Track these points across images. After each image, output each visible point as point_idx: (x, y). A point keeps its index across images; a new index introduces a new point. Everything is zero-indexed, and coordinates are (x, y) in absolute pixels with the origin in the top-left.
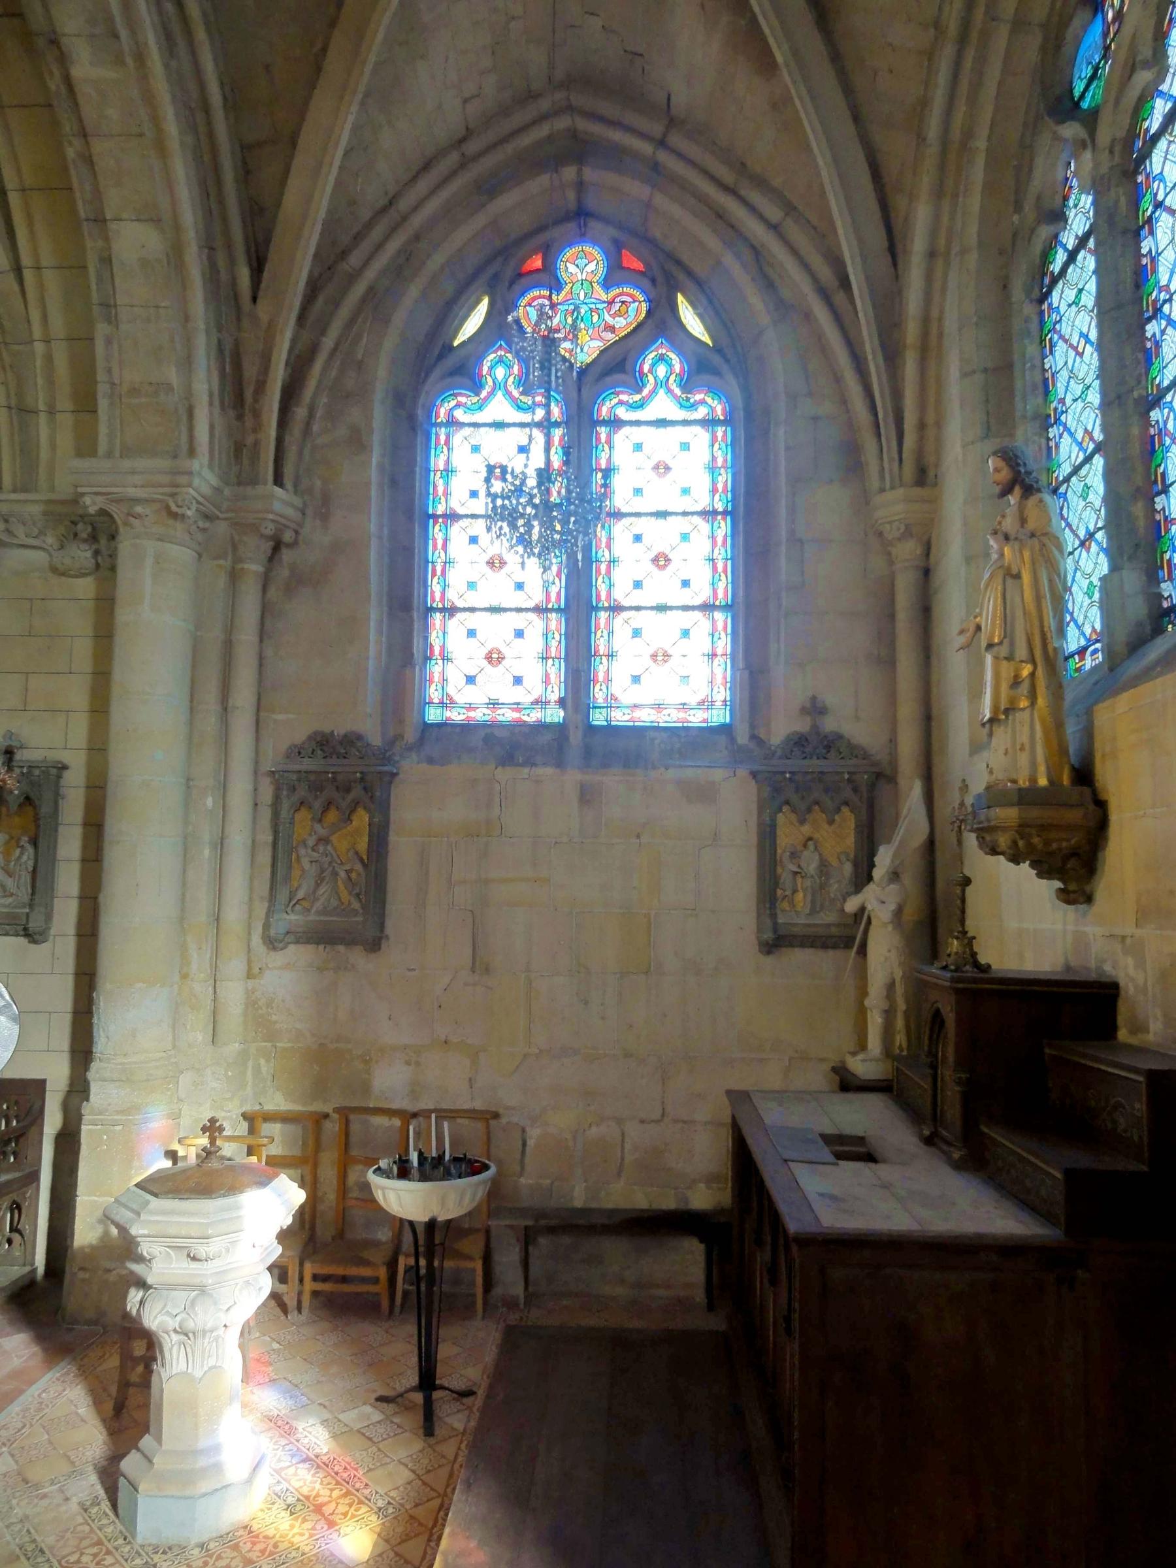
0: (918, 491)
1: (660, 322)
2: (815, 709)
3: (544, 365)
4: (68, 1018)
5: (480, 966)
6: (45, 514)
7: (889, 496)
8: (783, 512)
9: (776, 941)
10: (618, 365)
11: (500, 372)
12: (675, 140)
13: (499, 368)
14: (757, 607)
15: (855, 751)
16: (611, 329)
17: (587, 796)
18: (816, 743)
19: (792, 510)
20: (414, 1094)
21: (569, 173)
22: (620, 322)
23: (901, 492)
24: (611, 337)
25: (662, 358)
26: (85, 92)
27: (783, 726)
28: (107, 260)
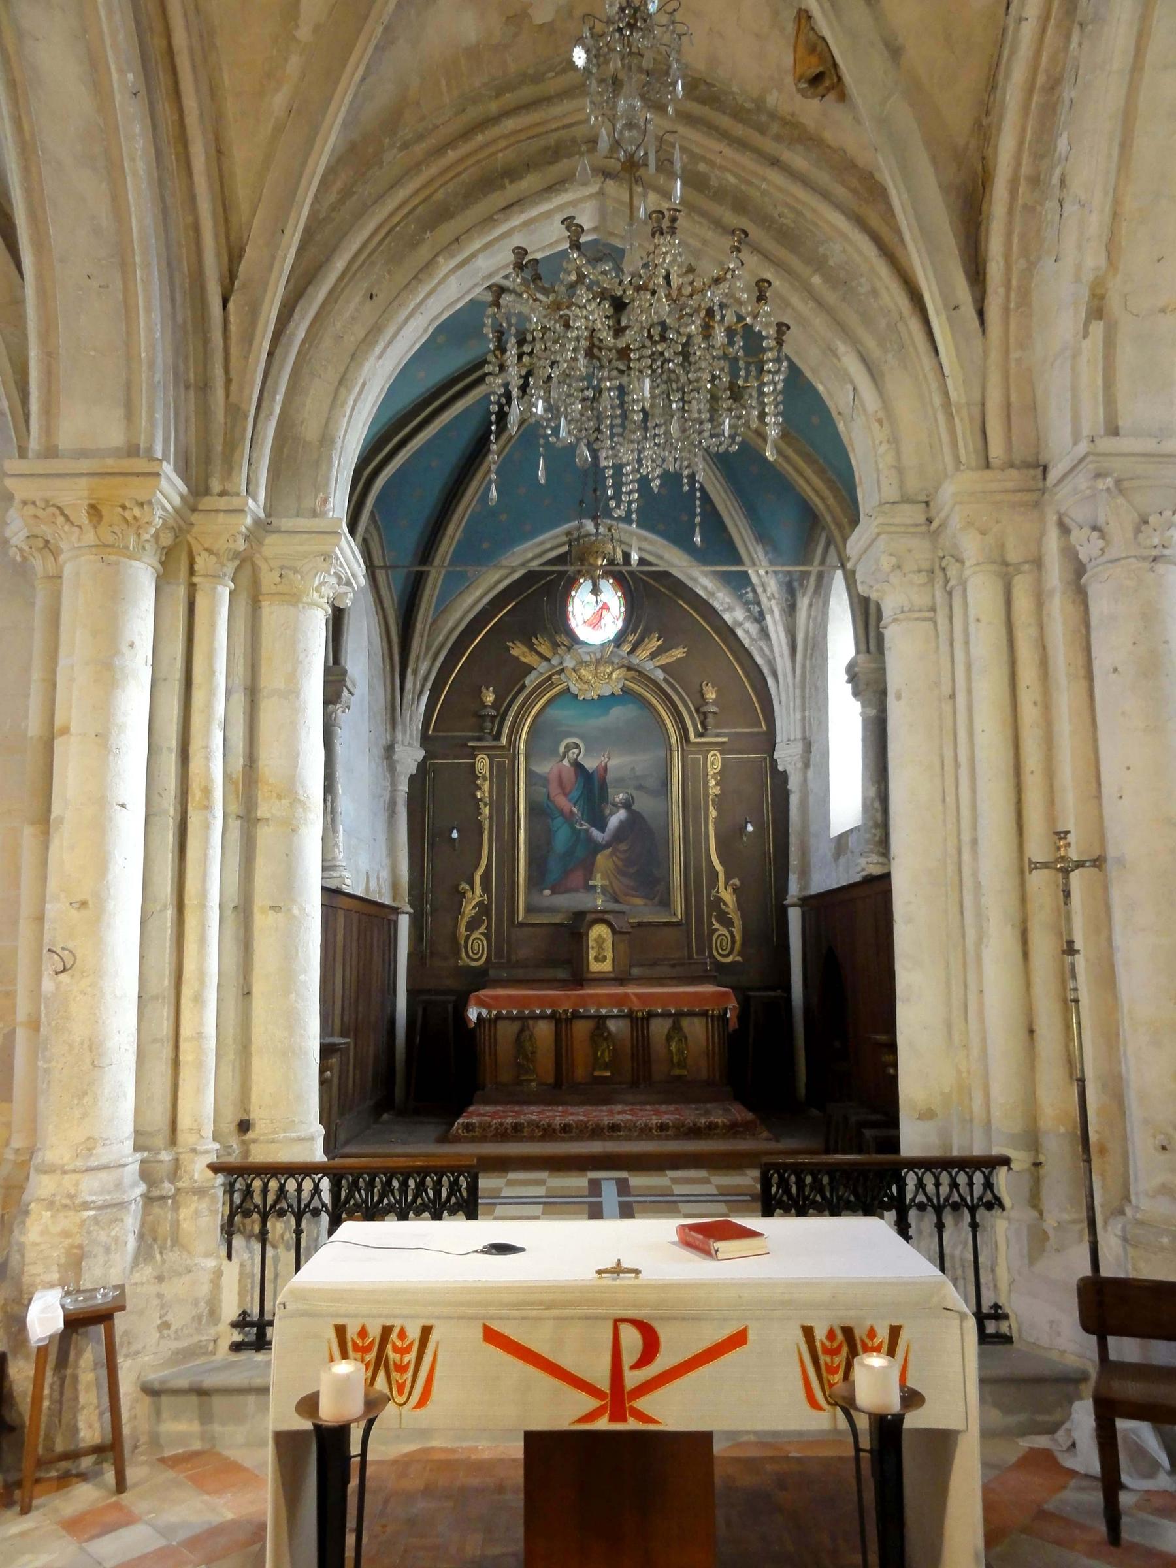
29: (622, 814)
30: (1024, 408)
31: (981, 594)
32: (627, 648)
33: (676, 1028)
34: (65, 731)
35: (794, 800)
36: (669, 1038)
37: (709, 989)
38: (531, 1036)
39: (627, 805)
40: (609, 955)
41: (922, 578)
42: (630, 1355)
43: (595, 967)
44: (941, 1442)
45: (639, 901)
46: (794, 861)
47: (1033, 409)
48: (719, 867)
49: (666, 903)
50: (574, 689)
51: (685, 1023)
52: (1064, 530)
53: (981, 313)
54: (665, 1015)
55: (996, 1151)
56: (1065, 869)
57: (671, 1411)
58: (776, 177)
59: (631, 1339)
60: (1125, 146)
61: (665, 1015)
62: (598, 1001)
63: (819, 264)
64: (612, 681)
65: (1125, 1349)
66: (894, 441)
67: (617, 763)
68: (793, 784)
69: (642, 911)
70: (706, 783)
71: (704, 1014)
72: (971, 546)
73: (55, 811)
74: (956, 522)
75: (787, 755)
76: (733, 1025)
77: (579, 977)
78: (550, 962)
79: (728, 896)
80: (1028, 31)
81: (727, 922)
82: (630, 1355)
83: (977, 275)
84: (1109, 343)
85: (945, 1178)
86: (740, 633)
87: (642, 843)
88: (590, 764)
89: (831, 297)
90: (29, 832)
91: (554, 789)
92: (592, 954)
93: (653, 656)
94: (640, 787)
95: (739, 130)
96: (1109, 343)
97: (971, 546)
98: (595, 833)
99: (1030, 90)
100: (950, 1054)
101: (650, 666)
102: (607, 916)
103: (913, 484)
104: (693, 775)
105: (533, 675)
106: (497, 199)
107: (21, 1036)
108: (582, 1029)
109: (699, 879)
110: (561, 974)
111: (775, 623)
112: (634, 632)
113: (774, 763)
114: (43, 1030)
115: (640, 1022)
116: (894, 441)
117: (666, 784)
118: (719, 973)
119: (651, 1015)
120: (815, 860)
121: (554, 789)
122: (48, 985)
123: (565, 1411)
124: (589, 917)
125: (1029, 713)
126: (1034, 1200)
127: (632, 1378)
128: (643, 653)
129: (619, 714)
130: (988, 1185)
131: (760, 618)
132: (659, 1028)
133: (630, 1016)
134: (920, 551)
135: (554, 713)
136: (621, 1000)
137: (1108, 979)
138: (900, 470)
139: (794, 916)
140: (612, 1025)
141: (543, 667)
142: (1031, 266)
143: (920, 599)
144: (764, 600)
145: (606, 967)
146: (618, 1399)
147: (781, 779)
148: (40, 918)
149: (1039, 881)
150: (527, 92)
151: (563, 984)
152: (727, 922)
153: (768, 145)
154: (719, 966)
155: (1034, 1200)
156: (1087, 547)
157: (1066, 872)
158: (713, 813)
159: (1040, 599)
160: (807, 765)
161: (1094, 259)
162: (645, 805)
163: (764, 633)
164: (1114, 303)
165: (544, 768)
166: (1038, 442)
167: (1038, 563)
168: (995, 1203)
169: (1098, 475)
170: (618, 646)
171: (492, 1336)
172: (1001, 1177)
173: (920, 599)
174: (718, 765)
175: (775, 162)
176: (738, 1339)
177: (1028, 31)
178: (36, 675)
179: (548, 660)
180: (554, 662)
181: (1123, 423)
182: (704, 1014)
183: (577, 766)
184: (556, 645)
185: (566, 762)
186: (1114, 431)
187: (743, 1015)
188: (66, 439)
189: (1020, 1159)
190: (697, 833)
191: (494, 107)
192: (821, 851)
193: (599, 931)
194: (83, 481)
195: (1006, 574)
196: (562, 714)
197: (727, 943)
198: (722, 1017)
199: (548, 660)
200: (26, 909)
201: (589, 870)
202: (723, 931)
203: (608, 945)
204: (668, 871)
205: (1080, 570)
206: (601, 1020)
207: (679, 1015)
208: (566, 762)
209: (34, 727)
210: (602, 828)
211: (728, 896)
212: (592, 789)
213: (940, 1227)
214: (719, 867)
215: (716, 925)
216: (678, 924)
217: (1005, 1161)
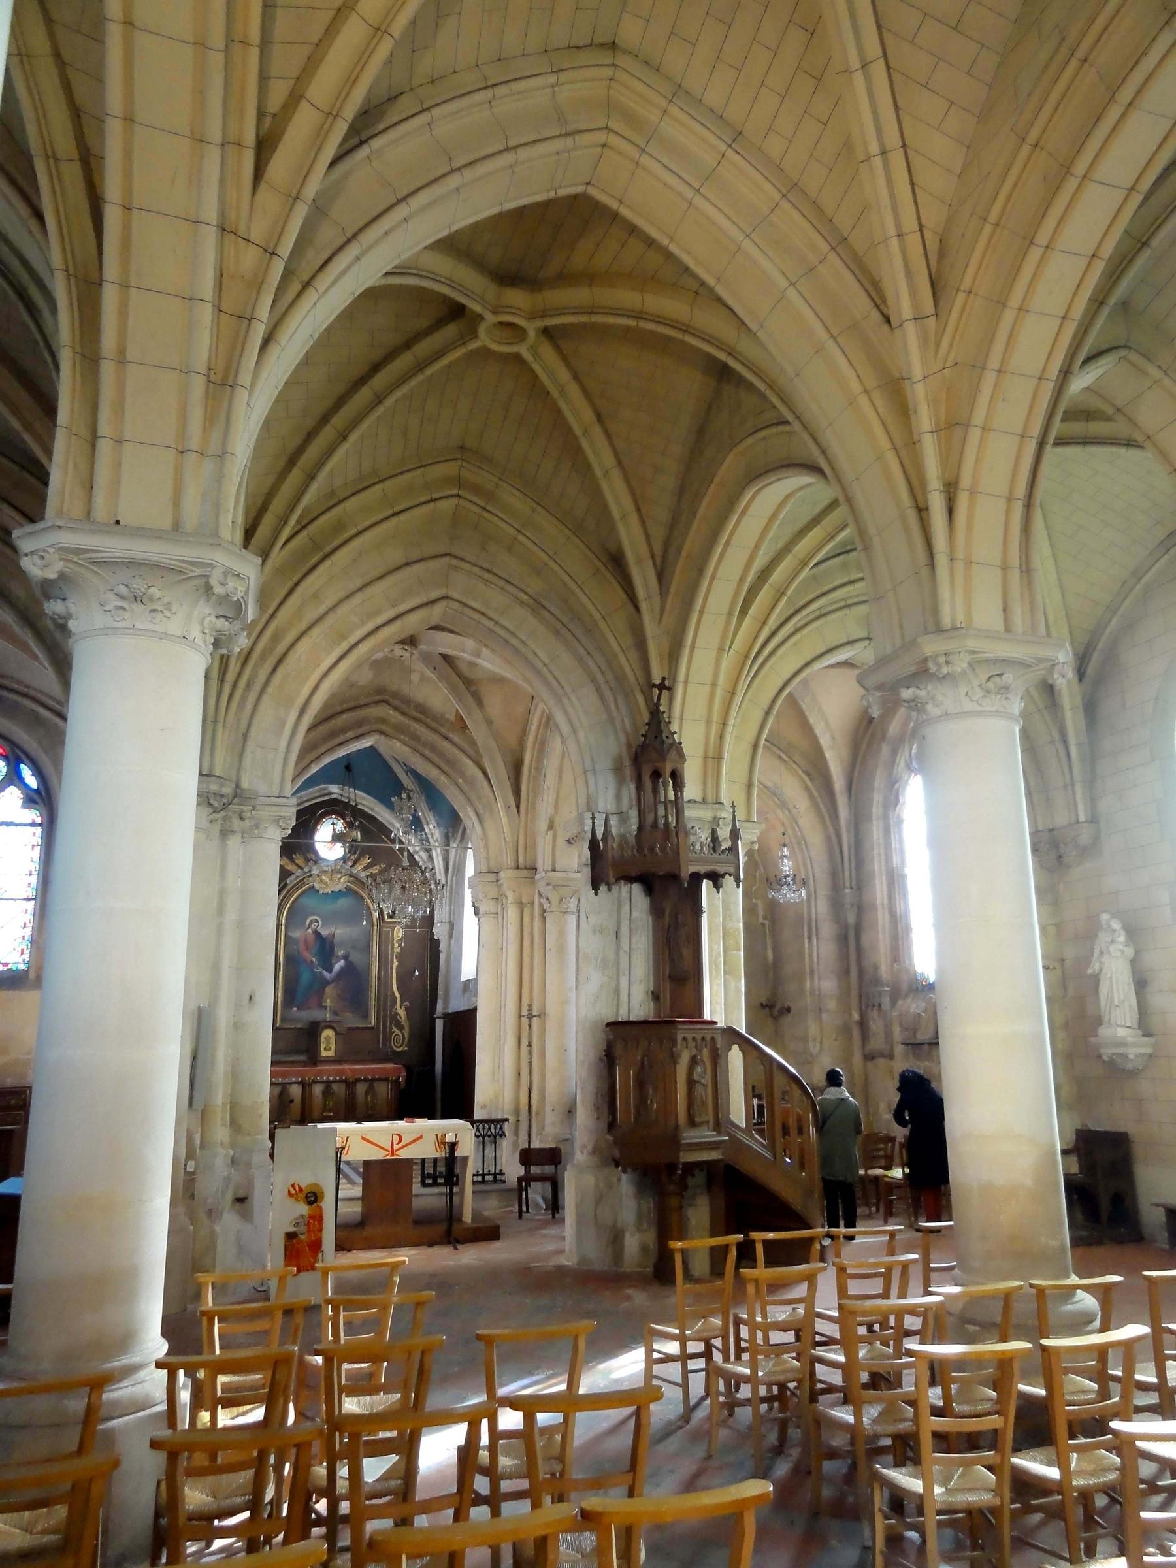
29: (342, 963)
30: (531, 846)
31: (512, 914)
32: (350, 864)
33: (370, 1090)
35: (442, 956)
36: (367, 1093)
37: (390, 1065)
38: (288, 1095)
39: (346, 957)
40: (333, 1047)
41: (493, 902)
42: (395, 1142)
43: (324, 1054)
44: (465, 1159)
45: (350, 1015)
46: (440, 992)
47: (534, 846)
48: (397, 995)
49: (366, 1016)
50: (317, 886)
51: (376, 1084)
52: (540, 895)
53: (518, 807)
54: (366, 1080)
55: (505, 1117)
56: (530, 1017)
57: (404, 1154)
58: (446, 744)
59: (396, 1138)
60: (560, 777)
61: (366, 1080)
62: (329, 1073)
63: (462, 775)
64: (342, 883)
65: (534, 1170)
66: (486, 847)
67: (340, 932)
68: (442, 947)
69: (351, 1020)
70: (393, 945)
71: (387, 1080)
72: (510, 895)
74: (505, 887)
75: (440, 930)
76: (403, 1086)
77: (314, 1058)
78: (299, 1052)
79: (402, 1012)
80: (534, 728)
81: (401, 1028)
82: (395, 1142)
83: (517, 792)
84: (555, 836)
85: (487, 1126)
86: (417, 857)
87: (354, 980)
88: (324, 932)
89: (466, 788)
91: (302, 946)
92: (323, 1046)
93: (365, 869)
94: (354, 947)
95: (434, 724)
96: (555, 836)
97: (510, 895)
98: (325, 973)
99: (535, 742)
100: (492, 1083)
101: (363, 874)
102: (335, 1025)
103: (492, 864)
104: (385, 940)
105: (293, 877)
106: (338, 740)
108: (318, 1090)
109: (385, 1001)
110: (302, 1058)
111: (437, 854)
112: (354, 853)
113: (432, 934)
115: (350, 1084)
116: (486, 847)
117: (369, 945)
118: (395, 1057)
119: (358, 1080)
120: (453, 993)
121: (302, 946)
123: (380, 1155)
124: (322, 1025)
125: (526, 959)
126: (516, 1133)
127: (396, 1147)
128: (359, 867)
129: (343, 902)
130: (501, 1128)
131: (428, 851)
132: (361, 1089)
133: (345, 1081)
134: (493, 892)
135: (305, 901)
136: (341, 1072)
137: (543, 1055)
138: (488, 859)
139: (439, 1025)
140: (335, 1087)
141: (298, 872)
142: (535, 796)
143: (493, 909)
144: (431, 841)
145: (331, 1053)
146: (392, 1152)
147: (435, 944)
149: (525, 1021)
150: (353, 704)
151: (304, 1064)
152: (401, 1028)
153: (443, 730)
154: (394, 1052)
155: (516, 1133)
156: (546, 906)
157: (530, 1019)
158: (396, 963)
159: (532, 919)
160: (451, 937)
161: (551, 811)
162: (355, 957)
163: (431, 857)
164: (556, 824)
165: (296, 934)
166: (535, 861)
167: (532, 904)
168: (503, 1135)
169: (548, 884)
170: (345, 862)
171: (363, 1138)
172: (506, 1126)
173: (493, 909)
174: (400, 935)
175: (446, 738)
176: (421, 1137)
177: (534, 728)
179: (302, 868)
180: (306, 870)
181: (558, 867)
182: (387, 1080)
183: (316, 933)
184: (308, 860)
185: (310, 931)
186: (554, 870)
187: (408, 1079)
189: (512, 1119)
190: (386, 975)
191: (339, 709)
192: (456, 990)
193: (328, 1033)
195: (521, 905)
196: (309, 902)
197: (400, 1040)
198: (397, 1081)
199: (302, 868)
201: (321, 994)
202: (398, 1032)
203: (333, 1041)
204: (368, 998)
205: (544, 911)
206: (328, 1084)
207: (373, 1080)
208: (310, 931)
210: (330, 972)
211: (402, 1012)
212: (325, 948)
213: (484, 1143)
214: (397, 995)
215: (394, 1029)
216: (373, 1028)
217: (507, 1120)
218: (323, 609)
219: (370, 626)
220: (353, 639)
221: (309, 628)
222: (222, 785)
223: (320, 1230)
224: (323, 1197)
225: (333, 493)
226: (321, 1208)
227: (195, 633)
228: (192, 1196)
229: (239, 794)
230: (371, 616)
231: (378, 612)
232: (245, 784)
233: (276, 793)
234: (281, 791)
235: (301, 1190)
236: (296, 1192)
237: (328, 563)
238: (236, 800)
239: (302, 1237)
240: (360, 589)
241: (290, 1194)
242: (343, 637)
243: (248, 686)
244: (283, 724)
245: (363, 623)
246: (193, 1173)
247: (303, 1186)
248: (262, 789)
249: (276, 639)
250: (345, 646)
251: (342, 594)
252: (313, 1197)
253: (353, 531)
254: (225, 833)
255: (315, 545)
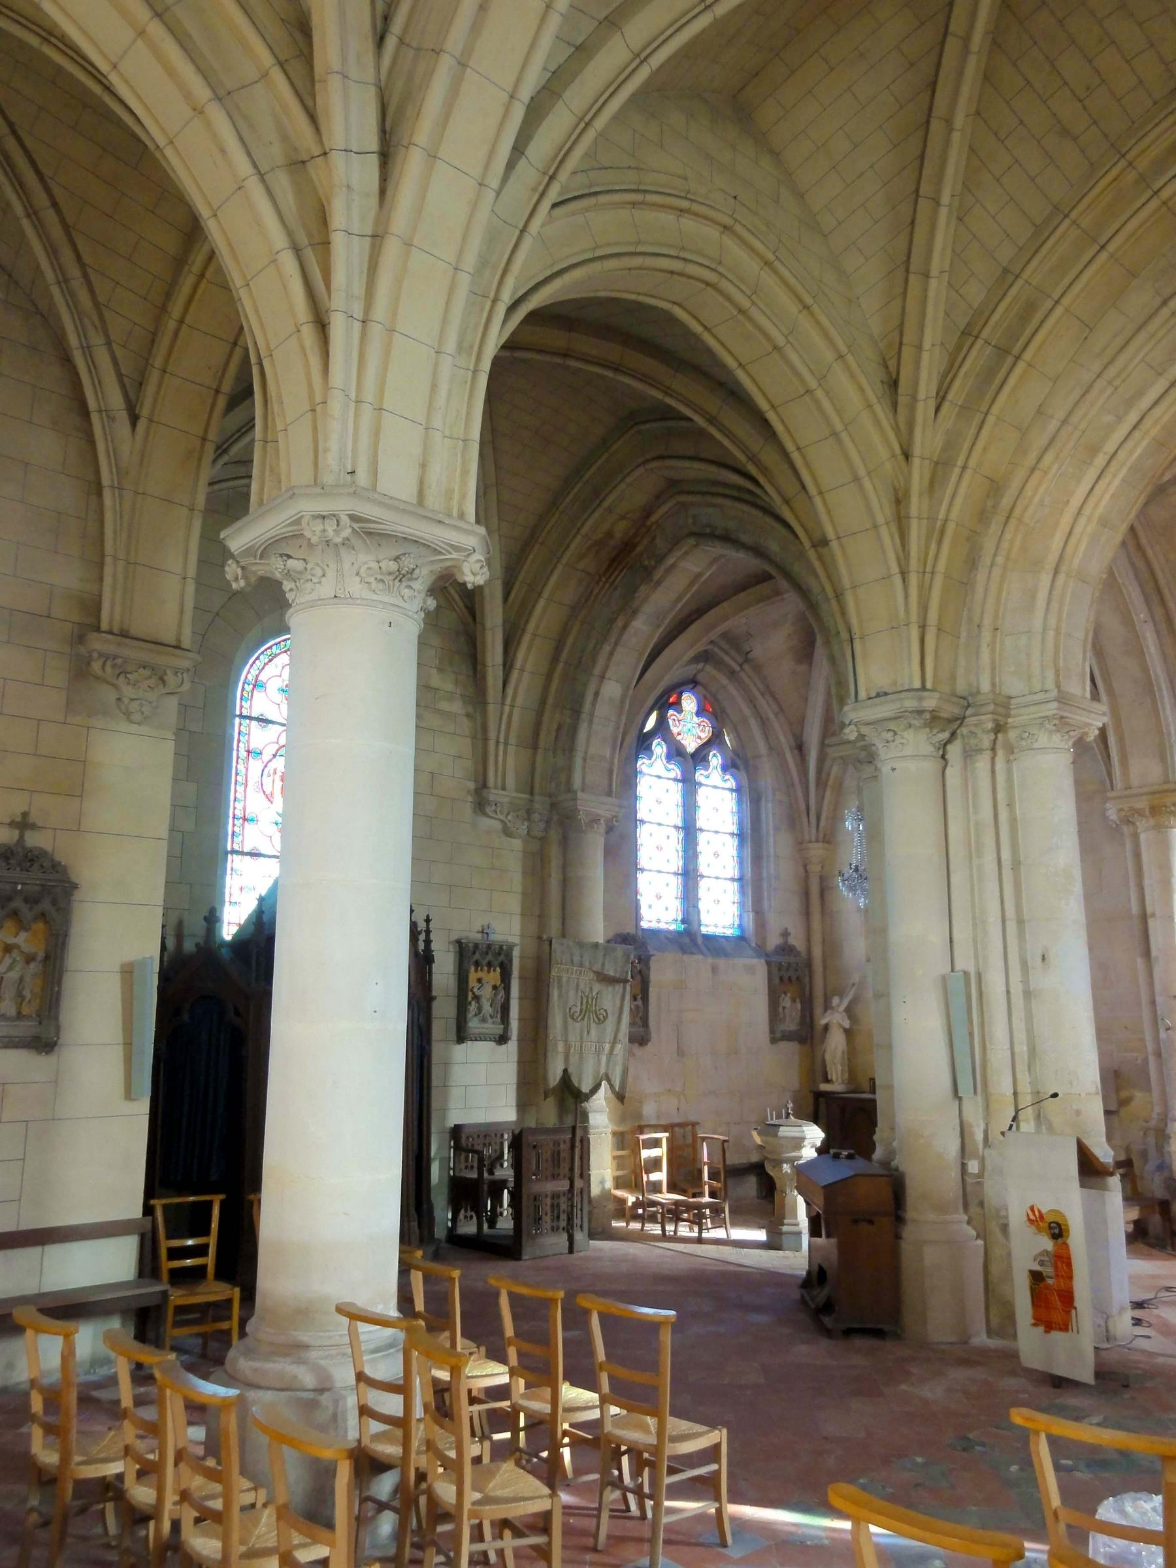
0: (826, 845)
1: (715, 740)
2: (785, 934)
3: (676, 752)
4: (515, 1086)
5: (681, 1053)
6: (511, 803)
7: (816, 845)
8: (771, 844)
9: (773, 1040)
10: (699, 757)
11: (659, 748)
12: (746, 666)
13: (659, 748)
14: (753, 883)
15: (799, 953)
16: (700, 738)
17: (714, 969)
18: (786, 949)
19: (775, 842)
20: (658, 1117)
21: (700, 666)
22: (703, 735)
23: (820, 845)
24: (701, 742)
25: (714, 755)
26: (630, 630)
27: (773, 941)
28: (597, 694)
34: (1153, 915)
73: (1154, 952)
90: (1140, 962)
107: (1151, 1059)
114: (1163, 1055)
122: (1163, 1035)
148: (1153, 1003)
178: (1132, 883)
188: (1135, 780)
194: (1144, 797)
200: (1145, 998)
209: (1135, 909)
218: (1053, 425)
219: (1133, 417)
220: (1110, 447)
221: (1039, 459)
222: (920, 699)
223: (1070, 1278)
224: (1068, 1231)
225: (1006, 271)
226: (1066, 1245)
227: (355, 587)
228: (981, 1204)
229: (968, 701)
230: (1129, 403)
231: (1140, 394)
232: (985, 686)
233: (1038, 687)
234: (1043, 684)
235: (1041, 1217)
236: (1036, 1219)
237: (1021, 365)
238: (968, 713)
239: (1050, 1282)
240: (1099, 376)
241: (1029, 1220)
242: (1094, 450)
243: (972, 563)
244: (1033, 597)
245: (1119, 419)
246: (981, 1175)
247: (1044, 1211)
248: (1013, 686)
249: (995, 488)
250: (1100, 460)
251: (1077, 393)
252: (1058, 1231)
253: (1049, 304)
254: (969, 755)
255: (1003, 352)
